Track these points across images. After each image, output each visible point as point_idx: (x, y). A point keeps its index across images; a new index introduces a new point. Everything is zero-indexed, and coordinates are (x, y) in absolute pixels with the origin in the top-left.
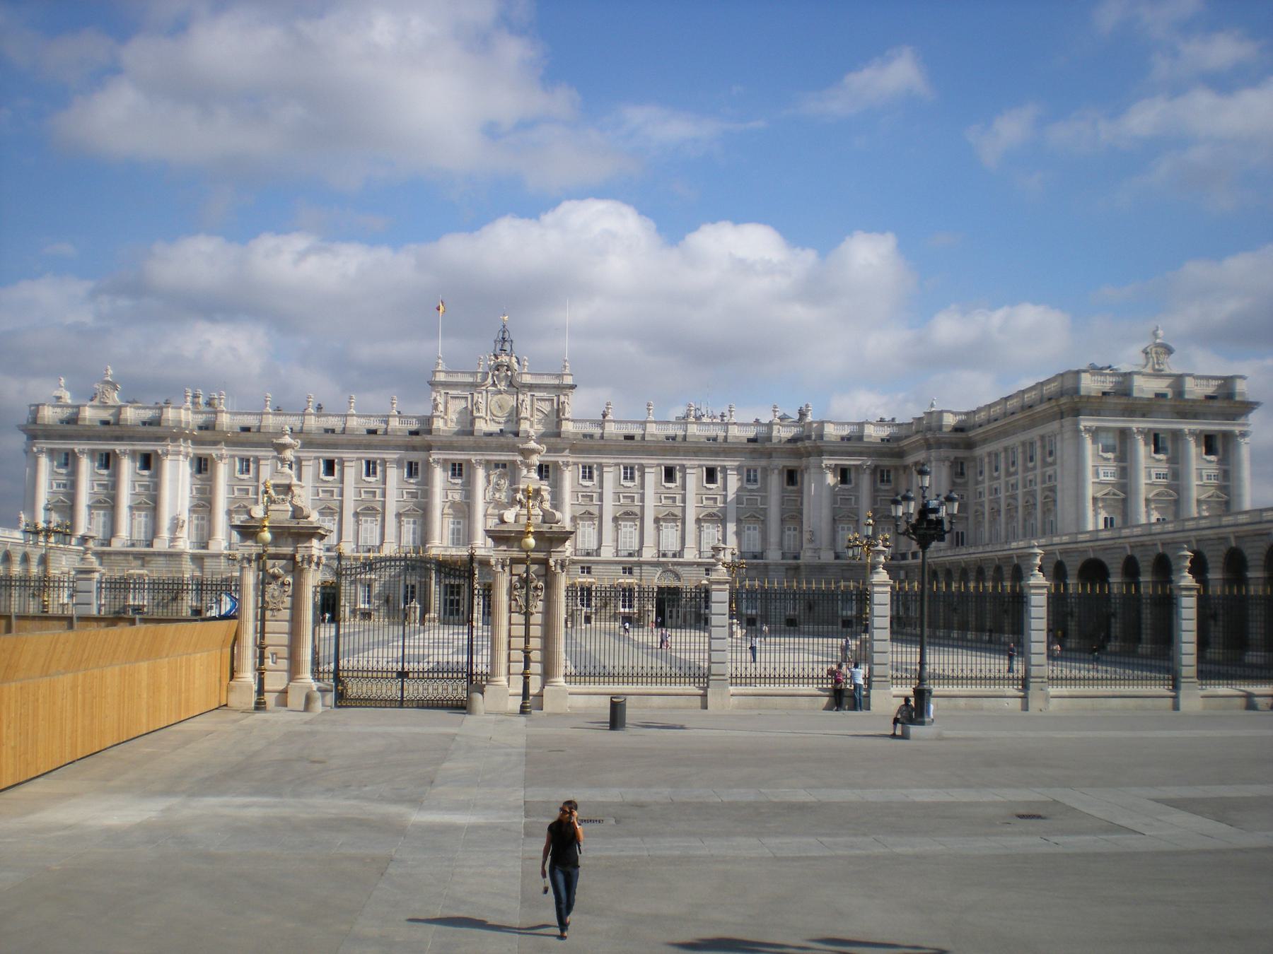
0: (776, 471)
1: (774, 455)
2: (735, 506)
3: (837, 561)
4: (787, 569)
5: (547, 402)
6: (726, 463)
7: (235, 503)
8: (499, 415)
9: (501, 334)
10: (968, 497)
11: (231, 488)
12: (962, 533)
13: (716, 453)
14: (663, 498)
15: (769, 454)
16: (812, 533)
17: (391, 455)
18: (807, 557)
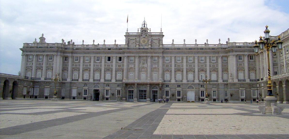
0: (220, 57)
1: (219, 53)
2: (209, 67)
3: (239, 82)
4: (224, 85)
5: (156, 40)
6: (206, 55)
7: (74, 69)
8: (144, 44)
9: (144, 22)
10: (277, 61)
11: (73, 65)
12: (276, 72)
13: (203, 53)
14: (188, 65)
15: (218, 53)
16: (231, 74)
17: (115, 55)
18: (230, 81)
